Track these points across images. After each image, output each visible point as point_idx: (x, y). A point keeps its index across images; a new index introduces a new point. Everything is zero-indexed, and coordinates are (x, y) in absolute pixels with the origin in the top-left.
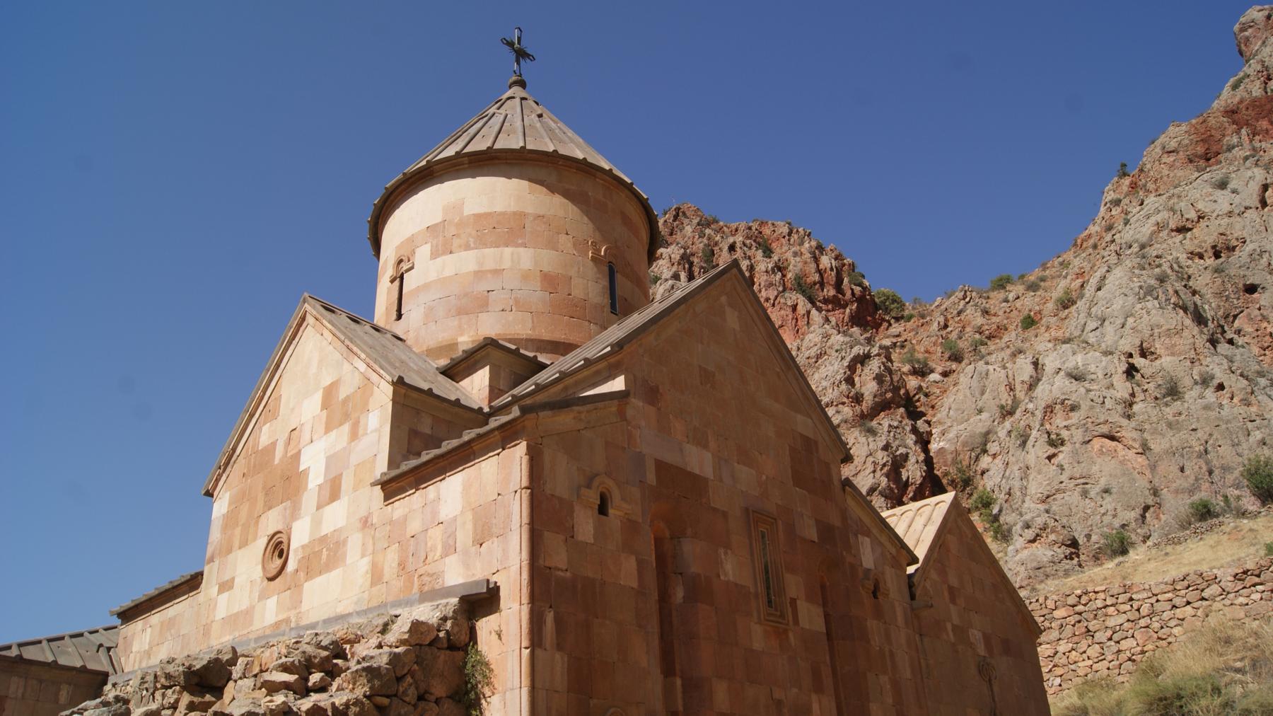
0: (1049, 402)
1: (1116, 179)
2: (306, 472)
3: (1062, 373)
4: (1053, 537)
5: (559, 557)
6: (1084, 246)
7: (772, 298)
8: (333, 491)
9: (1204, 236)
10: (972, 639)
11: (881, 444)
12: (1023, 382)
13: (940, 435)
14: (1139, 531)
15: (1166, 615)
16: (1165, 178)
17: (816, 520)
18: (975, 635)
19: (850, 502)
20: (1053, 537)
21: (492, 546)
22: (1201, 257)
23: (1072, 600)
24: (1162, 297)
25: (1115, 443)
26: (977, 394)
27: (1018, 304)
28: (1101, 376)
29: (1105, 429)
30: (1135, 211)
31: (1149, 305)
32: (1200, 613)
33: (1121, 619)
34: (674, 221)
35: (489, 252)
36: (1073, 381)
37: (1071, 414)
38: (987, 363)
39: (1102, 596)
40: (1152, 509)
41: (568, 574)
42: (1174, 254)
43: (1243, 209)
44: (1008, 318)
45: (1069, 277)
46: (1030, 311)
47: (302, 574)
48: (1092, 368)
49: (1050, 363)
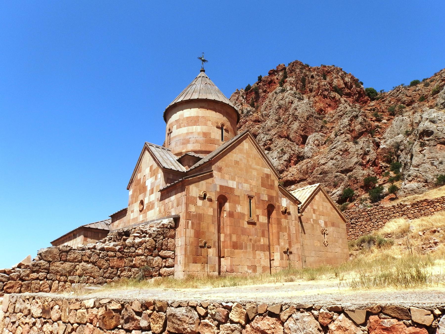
2: (147, 186)
3: (428, 120)
4: (419, 179)
8: (152, 192)
10: (320, 222)
11: (360, 148)
12: (416, 123)
18: (322, 222)
20: (419, 179)
21: (180, 207)
23: (366, 210)
26: (399, 127)
27: (420, 92)
36: (432, 123)
38: (403, 116)
41: (195, 213)
44: (415, 98)
45: (439, 81)
46: (424, 95)
47: (147, 210)
48: (440, 118)
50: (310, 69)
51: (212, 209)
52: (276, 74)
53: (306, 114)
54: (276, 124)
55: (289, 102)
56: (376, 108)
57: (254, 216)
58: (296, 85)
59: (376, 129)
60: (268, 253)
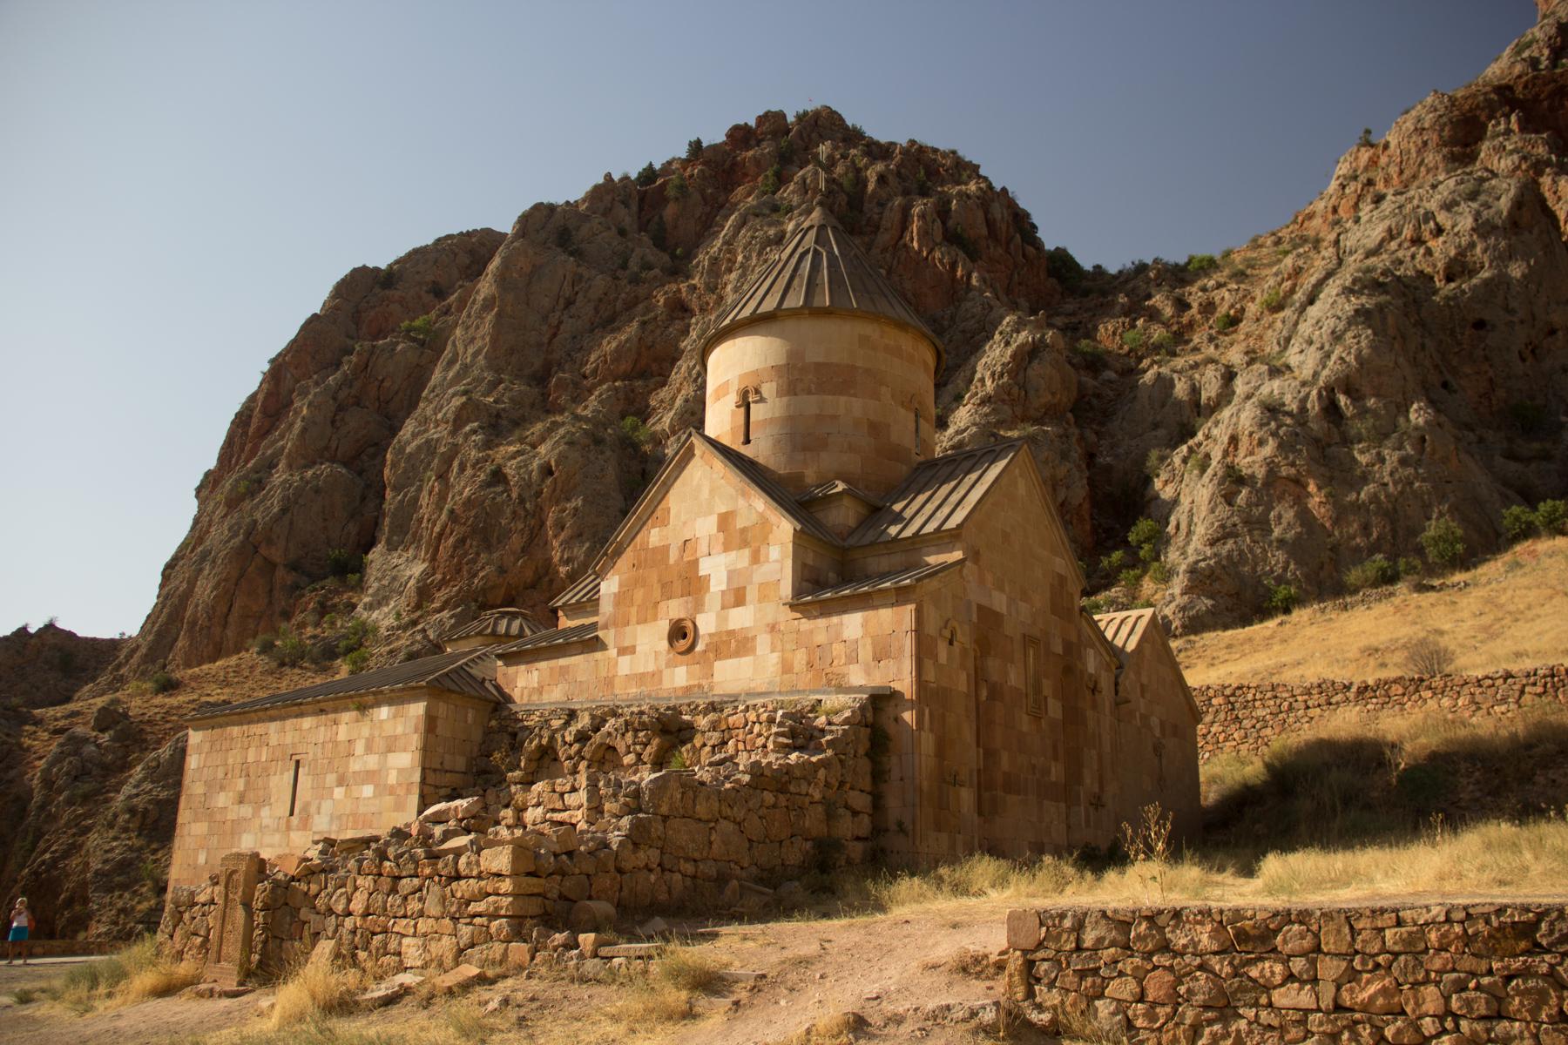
3: (1254, 399)
5: (930, 675)
6: (1306, 223)
18: (1155, 721)
19: (1084, 623)
39: (1253, 691)
48: (1288, 398)
51: (963, 677)
56: (1080, 322)
60: (1063, 805)
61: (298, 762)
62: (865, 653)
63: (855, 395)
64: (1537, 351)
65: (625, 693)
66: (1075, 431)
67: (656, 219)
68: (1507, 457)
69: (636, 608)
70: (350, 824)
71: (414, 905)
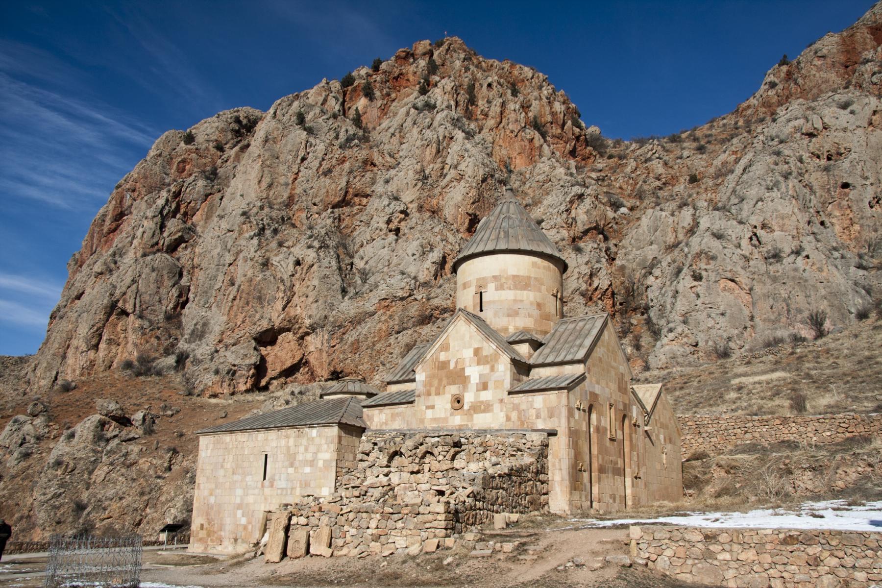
0: (698, 251)
1: (777, 65)
2: (469, 377)
4: (685, 340)
5: (572, 425)
6: (744, 114)
7: (516, 131)
8: (484, 387)
9: (824, 143)
12: (683, 227)
13: (623, 255)
14: (738, 342)
15: (730, 431)
16: (812, 77)
17: (623, 403)
18: (662, 437)
21: (555, 419)
22: (818, 157)
23: (695, 419)
24: (783, 189)
25: (733, 284)
28: (734, 238)
29: (729, 275)
30: (782, 114)
31: (774, 194)
32: (743, 432)
33: (713, 430)
34: (446, 54)
35: (519, 292)
36: (716, 239)
37: (711, 262)
38: (661, 210)
40: (748, 329)
42: (801, 152)
43: (854, 127)
45: (727, 152)
47: (472, 412)
49: (704, 223)
50: (480, 63)
52: (411, 60)
53: (481, 172)
54: (418, 180)
55: (445, 137)
57: (613, 431)
58: (455, 96)
59: (608, 224)
61: (266, 456)
62: (544, 414)
63: (530, 290)
64: (880, 202)
65: (429, 426)
66: (603, 245)
67: (354, 108)
68: (858, 268)
69: (434, 388)
70: (298, 485)
71: (400, 524)
